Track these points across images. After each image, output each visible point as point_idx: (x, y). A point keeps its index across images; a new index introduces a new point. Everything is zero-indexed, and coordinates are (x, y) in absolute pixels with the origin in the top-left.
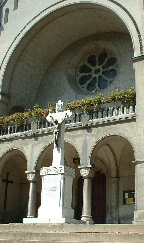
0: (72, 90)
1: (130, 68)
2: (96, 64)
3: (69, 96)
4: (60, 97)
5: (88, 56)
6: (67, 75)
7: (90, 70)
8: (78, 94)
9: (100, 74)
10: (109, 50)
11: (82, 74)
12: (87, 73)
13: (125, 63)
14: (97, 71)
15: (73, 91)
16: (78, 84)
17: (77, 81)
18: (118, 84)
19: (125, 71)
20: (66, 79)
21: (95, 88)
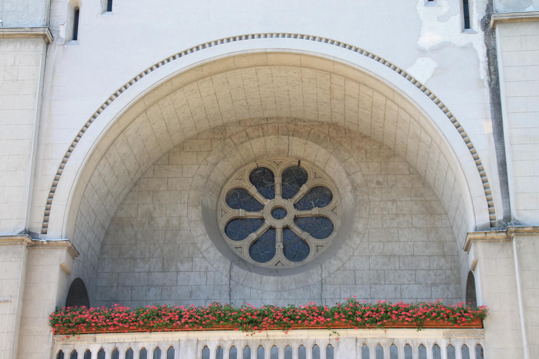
0: (217, 251)
1: (380, 226)
2: (291, 198)
3: (207, 268)
4: (179, 264)
5: (253, 166)
6: (200, 208)
7: (260, 207)
8: (235, 267)
9: (288, 220)
10: (314, 164)
11: (236, 210)
12: (249, 210)
13: (368, 210)
14: (278, 212)
15: (220, 254)
16: (224, 235)
17: (222, 227)
18: (349, 259)
19: (367, 231)
20: (198, 219)
21: (274, 254)
